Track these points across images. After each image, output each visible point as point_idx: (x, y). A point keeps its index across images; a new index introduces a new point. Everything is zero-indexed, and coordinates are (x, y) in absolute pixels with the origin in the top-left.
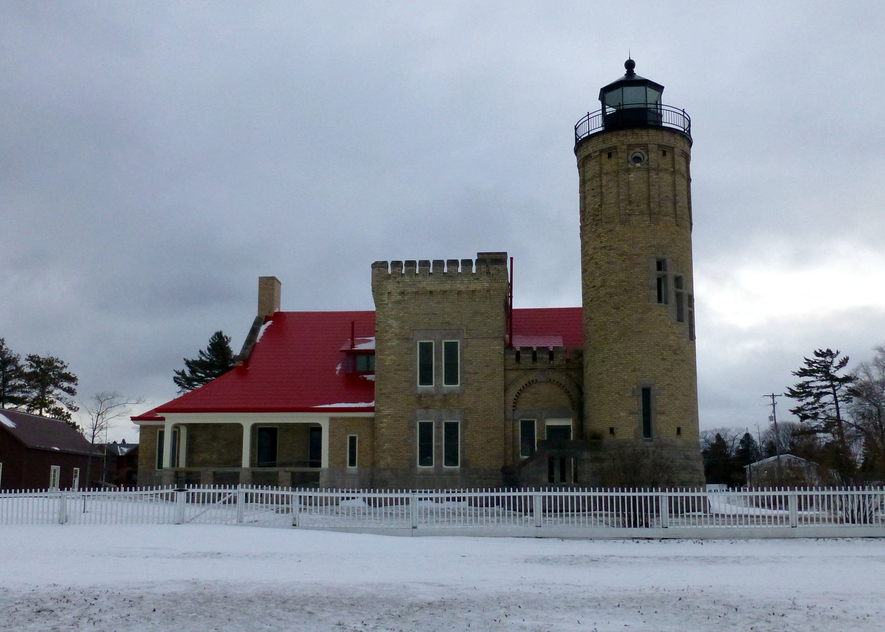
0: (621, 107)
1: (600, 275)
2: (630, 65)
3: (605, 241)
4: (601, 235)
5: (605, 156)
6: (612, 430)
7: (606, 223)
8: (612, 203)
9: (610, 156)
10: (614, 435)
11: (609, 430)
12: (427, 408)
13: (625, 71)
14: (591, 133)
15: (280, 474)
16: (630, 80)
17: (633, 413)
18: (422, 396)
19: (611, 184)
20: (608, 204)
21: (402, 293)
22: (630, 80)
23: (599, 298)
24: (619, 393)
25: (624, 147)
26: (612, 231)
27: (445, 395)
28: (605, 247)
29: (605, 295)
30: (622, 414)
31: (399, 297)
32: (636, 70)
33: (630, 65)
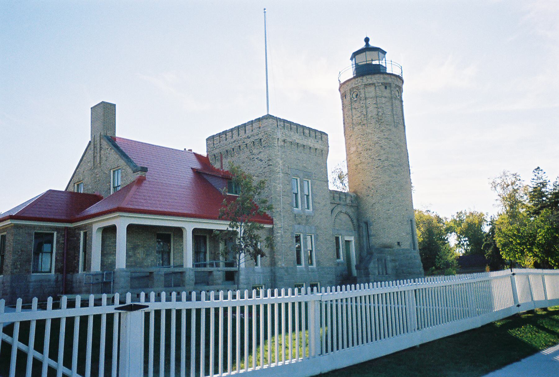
0: (391, 63)
1: (384, 153)
2: (367, 40)
5: (383, 87)
6: (399, 243)
7: (387, 125)
9: (386, 88)
10: (400, 246)
13: (364, 44)
15: (215, 273)
16: (368, 49)
17: (408, 234)
18: (297, 215)
19: (387, 104)
20: (387, 114)
21: (284, 141)
22: (368, 49)
23: (384, 166)
27: (307, 216)
28: (387, 138)
31: (282, 143)
33: (367, 40)
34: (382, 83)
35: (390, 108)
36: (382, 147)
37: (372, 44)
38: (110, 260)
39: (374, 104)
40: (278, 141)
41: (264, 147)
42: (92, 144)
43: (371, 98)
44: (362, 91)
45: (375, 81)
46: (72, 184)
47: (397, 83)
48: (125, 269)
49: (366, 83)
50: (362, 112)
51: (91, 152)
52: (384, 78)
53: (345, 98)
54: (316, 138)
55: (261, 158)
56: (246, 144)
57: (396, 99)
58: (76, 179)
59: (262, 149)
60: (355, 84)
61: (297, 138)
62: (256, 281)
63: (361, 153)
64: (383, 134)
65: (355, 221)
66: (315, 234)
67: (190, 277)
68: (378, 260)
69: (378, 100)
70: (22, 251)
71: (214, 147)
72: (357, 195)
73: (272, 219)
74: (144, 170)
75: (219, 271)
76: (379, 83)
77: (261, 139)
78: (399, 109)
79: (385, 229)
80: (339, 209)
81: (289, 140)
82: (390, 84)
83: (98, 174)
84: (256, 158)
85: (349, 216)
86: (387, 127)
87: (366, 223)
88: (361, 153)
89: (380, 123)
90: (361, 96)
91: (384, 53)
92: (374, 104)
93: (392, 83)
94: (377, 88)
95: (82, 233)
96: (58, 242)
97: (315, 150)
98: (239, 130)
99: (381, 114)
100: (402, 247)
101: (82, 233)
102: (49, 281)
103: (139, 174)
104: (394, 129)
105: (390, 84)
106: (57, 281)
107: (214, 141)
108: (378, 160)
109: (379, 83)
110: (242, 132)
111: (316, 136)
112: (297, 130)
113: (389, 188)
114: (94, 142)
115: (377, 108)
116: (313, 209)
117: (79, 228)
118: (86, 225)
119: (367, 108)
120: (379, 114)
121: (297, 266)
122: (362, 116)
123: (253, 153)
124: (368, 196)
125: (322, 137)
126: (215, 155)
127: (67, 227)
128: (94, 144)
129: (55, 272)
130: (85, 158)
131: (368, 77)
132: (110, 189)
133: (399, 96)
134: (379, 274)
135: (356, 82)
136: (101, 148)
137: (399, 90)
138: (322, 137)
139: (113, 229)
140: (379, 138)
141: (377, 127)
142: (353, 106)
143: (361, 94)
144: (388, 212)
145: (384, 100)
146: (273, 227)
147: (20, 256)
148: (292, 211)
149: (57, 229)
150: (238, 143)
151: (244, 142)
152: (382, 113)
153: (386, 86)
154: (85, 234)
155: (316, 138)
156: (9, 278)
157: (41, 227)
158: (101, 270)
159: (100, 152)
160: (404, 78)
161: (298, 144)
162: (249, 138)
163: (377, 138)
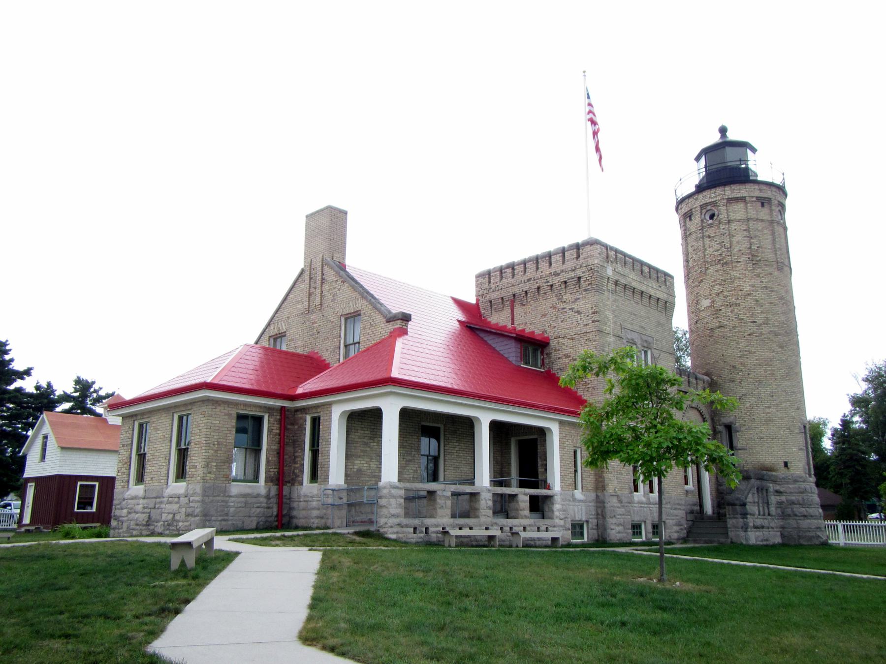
2: (723, 131)
6: (786, 464)
7: (766, 265)
9: (763, 205)
10: (788, 469)
13: (719, 135)
19: (765, 232)
20: (766, 249)
21: (616, 283)
23: (761, 334)
24: (789, 429)
25: (776, 202)
28: (766, 288)
29: (769, 333)
33: (723, 131)
34: (757, 197)
35: (770, 237)
36: (757, 301)
37: (732, 136)
38: (356, 467)
39: (744, 230)
40: (608, 282)
43: (739, 221)
44: (723, 209)
48: (397, 484)
49: (730, 197)
50: (723, 242)
51: (303, 286)
52: (761, 190)
53: (690, 219)
54: (658, 281)
55: (579, 309)
56: (552, 286)
58: (273, 331)
59: (581, 294)
60: (710, 197)
61: (633, 278)
63: (720, 310)
64: (759, 280)
67: (486, 501)
69: (751, 225)
70: (218, 444)
72: (712, 379)
76: (753, 197)
77: (579, 278)
78: (783, 240)
79: (762, 438)
81: (623, 281)
82: (769, 200)
83: (316, 323)
84: (570, 309)
86: (766, 269)
87: (729, 428)
88: (720, 310)
89: (754, 262)
91: (754, 150)
92: (744, 230)
93: (773, 198)
96: (270, 431)
99: (756, 248)
101: (308, 419)
102: (258, 496)
103: (398, 324)
104: (776, 273)
105: (770, 199)
106: (268, 497)
108: (751, 322)
110: (543, 265)
111: (658, 277)
112: (633, 265)
114: (310, 269)
117: (304, 410)
118: (317, 407)
119: (731, 236)
122: (723, 249)
123: (563, 300)
124: (733, 381)
126: (491, 302)
127: (285, 407)
128: (310, 274)
129: (265, 482)
130: (291, 296)
131: (733, 187)
135: (713, 195)
136: (323, 279)
138: (665, 279)
139: (375, 415)
140: (753, 286)
142: (707, 234)
143: (721, 214)
144: (768, 410)
145: (760, 225)
147: (216, 451)
149: (269, 409)
150: (537, 283)
151: (548, 282)
152: (758, 246)
153: (763, 202)
154: (316, 422)
155: (658, 281)
156: (198, 488)
157: (247, 405)
158: (345, 483)
159: (322, 286)
160: (788, 189)
161: (634, 288)
162: (559, 274)
163: (749, 286)
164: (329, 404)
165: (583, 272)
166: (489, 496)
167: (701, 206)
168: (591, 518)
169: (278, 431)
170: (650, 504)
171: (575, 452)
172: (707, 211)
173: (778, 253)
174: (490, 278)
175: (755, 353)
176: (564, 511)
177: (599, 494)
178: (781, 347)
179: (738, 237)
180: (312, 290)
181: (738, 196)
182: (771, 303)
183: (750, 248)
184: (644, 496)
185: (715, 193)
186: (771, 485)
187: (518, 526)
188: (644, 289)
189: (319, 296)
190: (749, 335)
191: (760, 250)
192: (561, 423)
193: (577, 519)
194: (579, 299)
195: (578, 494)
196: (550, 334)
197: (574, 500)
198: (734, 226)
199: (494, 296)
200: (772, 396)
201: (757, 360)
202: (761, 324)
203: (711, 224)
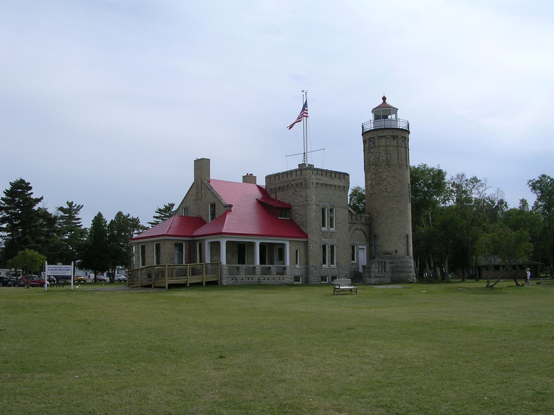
2: (384, 99)
3: (393, 174)
4: (391, 171)
6: (396, 251)
7: (393, 166)
8: (395, 159)
9: (394, 139)
10: (397, 253)
11: (395, 251)
12: (325, 238)
13: (382, 101)
14: (386, 127)
15: (272, 268)
17: (404, 245)
25: (400, 137)
26: (396, 170)
28: (393, 176)
29: (393, 196)
30: (400, 245)
31: (316, 185)
32: (386, 101)
33: (384, 99)
34: (391, 136)
39: (385, 151)
41: (304, 188)
42: (195, 184)
43: (383, 146)
45: (386, 134)
46: (181, 208)
47: (403, 135)
48: (226, 265)
49: (380, 135)
53: (366, 144)
54: (340, 178)
56: (292, 185)
57: (401, 147)
58: (184, 206)
59: (302, 189)
60: (372, 135)
61: (325, 180)
62: (297, 274)
64: (390, 173)
65: (367, 235)
66: (336, 245)
67: (258, 269)
68: (379, 262)
69: (388, 148)
71: (271, 183)
72: (370, 216)
73: (308, 236)
74: (231, 206)
75: (274, 267)
76: (389, 136)
77: (302, 183)
80: (355, 227)
82: (397, 136)
83: (199, 205)
85: (363, 231)
88: (374, 186)
89: (388, 165)
90: (376, 144)
92: (385, 151)
93: (398, 135)
94: (387, 139)
95: (198, 244)
97: (339, 187)
98: (287, 175)
99: (389, 159)
100: (399, 254)
101: (198, 244)
103: (228, 209)
105: (397, 136)
107: (270, 179)
108: (386, 192)
109: (389, 136)
110: (289, 176)
111: (340, 177)
112: (326, 174)
113: (392, 212)
115: (386, 154)
116: (336, 228)
117: (197, 241)
119: (379, 153)
120: (388, 158)
121: (323, 265)
122: (376, 159)
124: (377, 217)
125: (344, 177)
132: (208, 215)
133: (404, 144)
134: (379, 272)
135: (373, 134)
137: (404, 140)
138: (344, 177)
139: (218, 244)
141: (386, 168)
142: (371, 151)
143: (376, 143)
144: (390, 229)
145: (392, 148)
146: (308, 240)
148: (321, 230)
149: (185, 241)
151: (291, 183)
152: (390, 158)
154: (200, 245)
155: (340, 178)
157: (177, 240)
159: (201, 190)
162: (294, 181)
163: (386, 176)
164: (205, 239)
165: (303, 181)
166: (259, 268)
167: (369, 138)
168: (303, 275)
169: (188, 248)
170: (331, 269)
171: (297, 252)
172: (371, 141)
173: (400, 160)
174: (270, 179)
175: (386, 205)
176: (291, 272)
177: (307, 266)
178: (398, 202)
179: (383, 154)
180: (198, 191)
181: (383, 135)
182: (395, 183)
183: (387, 159)
184: (328, 266)
185: (374, 133)
186: (387, 260)
187: (271, 278)
188: (332, 183)
189: (200, 194)
190: (385, 197)
191: (391, 159)
192: (290, 241)
193: (297, 275)
194: (301, 191)
195: (297, 266)
196: (292, 204)
197: (295, 268)
198: (381, 149)
199: (272, 187)
200: (392, 223)
201: (387, 208)
202: (389, 192)
203: (372, 147)
